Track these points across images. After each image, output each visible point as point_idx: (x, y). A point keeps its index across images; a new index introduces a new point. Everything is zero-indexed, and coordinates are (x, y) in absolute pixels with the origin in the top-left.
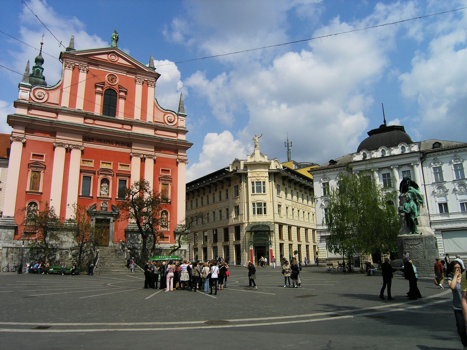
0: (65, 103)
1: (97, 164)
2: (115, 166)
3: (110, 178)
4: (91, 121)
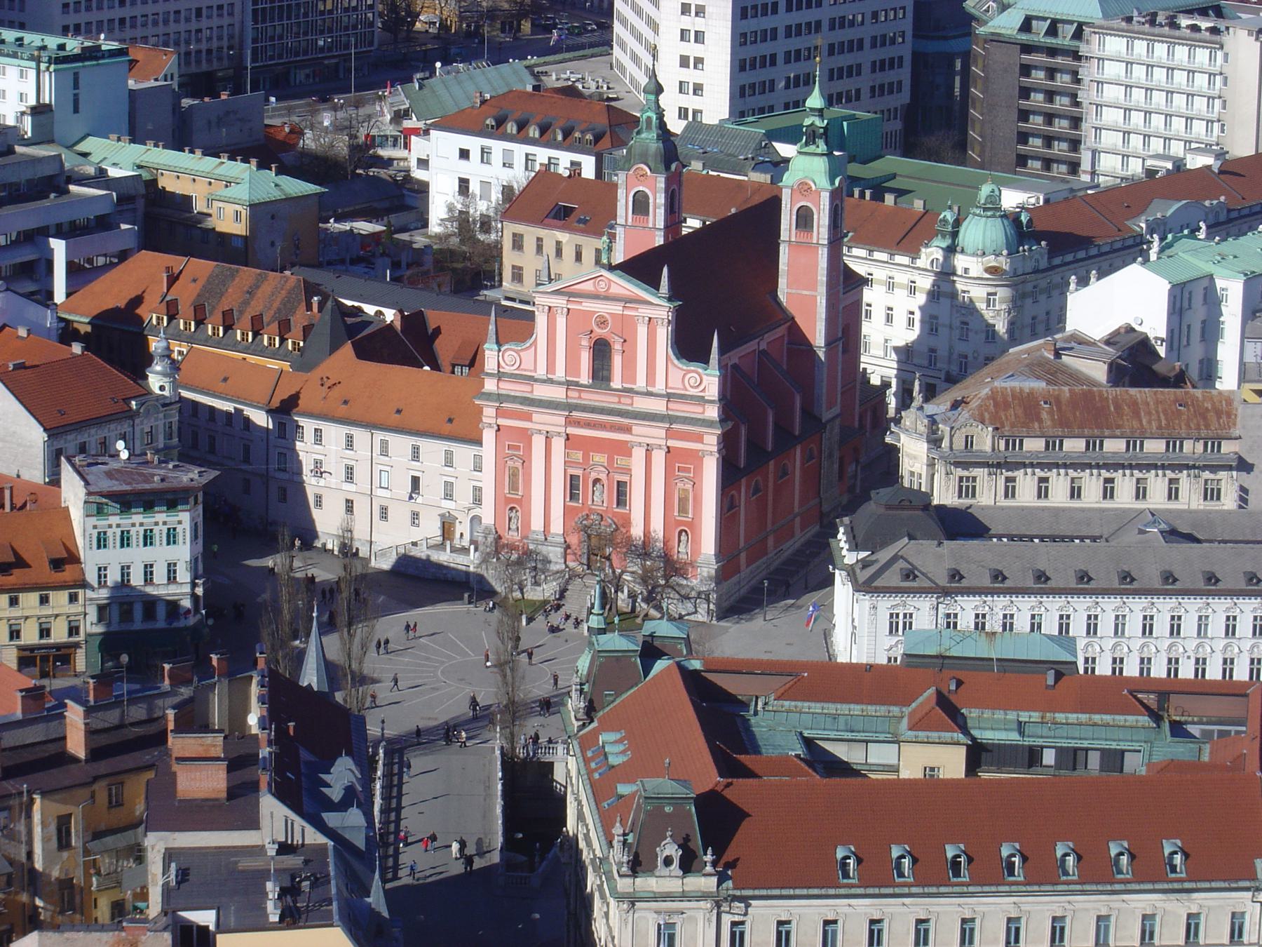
0: (541, 372)
1: (586, 457)
2: (610, 460)
3: (603, 476)
4: (576, 394)
